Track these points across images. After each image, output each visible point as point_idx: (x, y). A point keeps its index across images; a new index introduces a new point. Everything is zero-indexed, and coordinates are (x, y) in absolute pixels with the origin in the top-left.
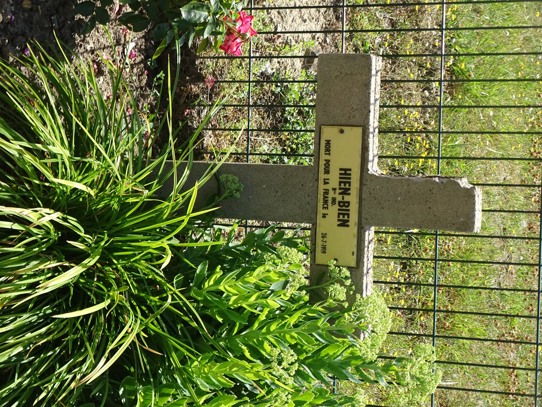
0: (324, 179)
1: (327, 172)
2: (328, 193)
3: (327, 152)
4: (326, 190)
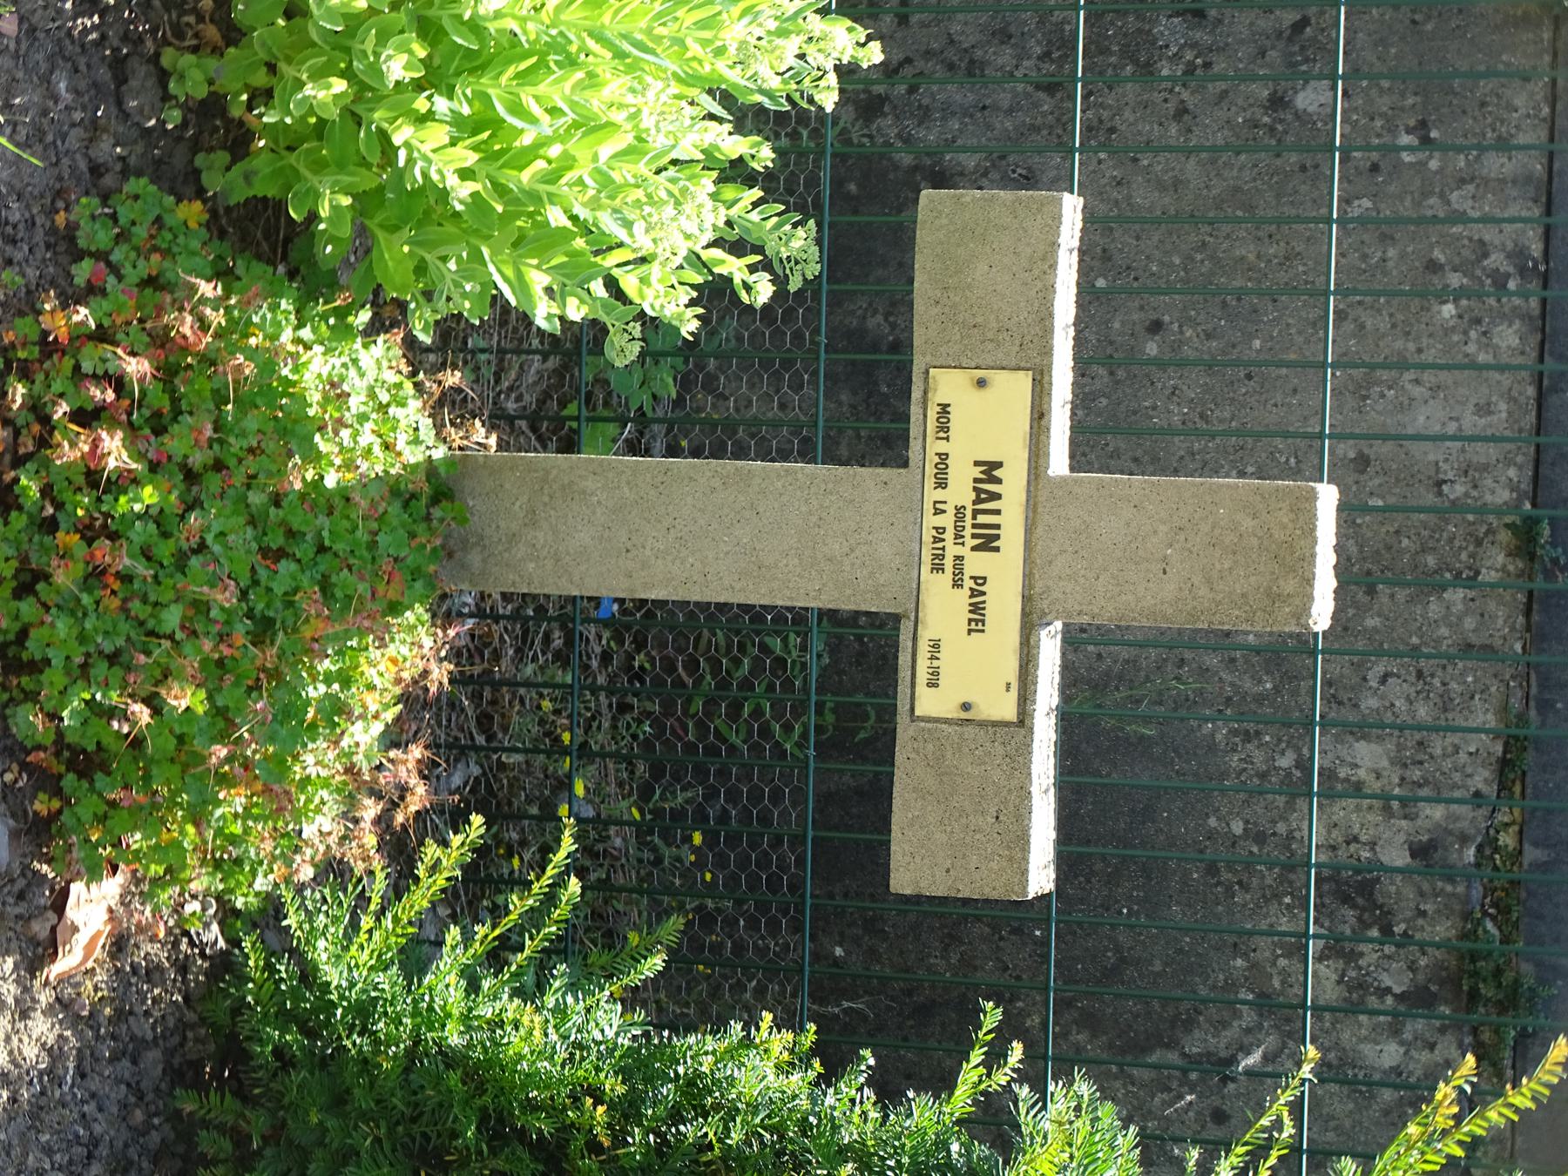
1: (942, 484)
3: (942, 435)
4: (936, 528)
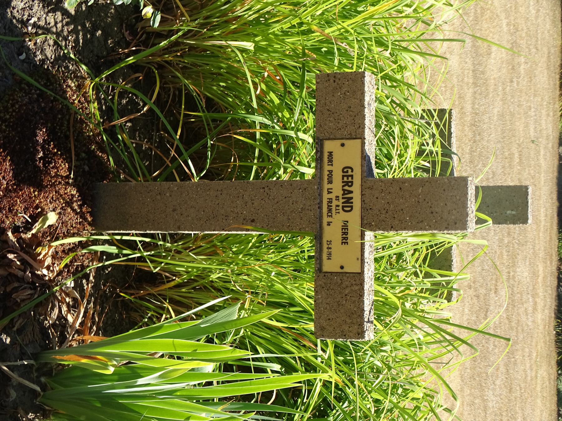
0: (328, 189)
1: (330, 182)
2: (331, 202)
3: (330, 163)
4: (330, 199)
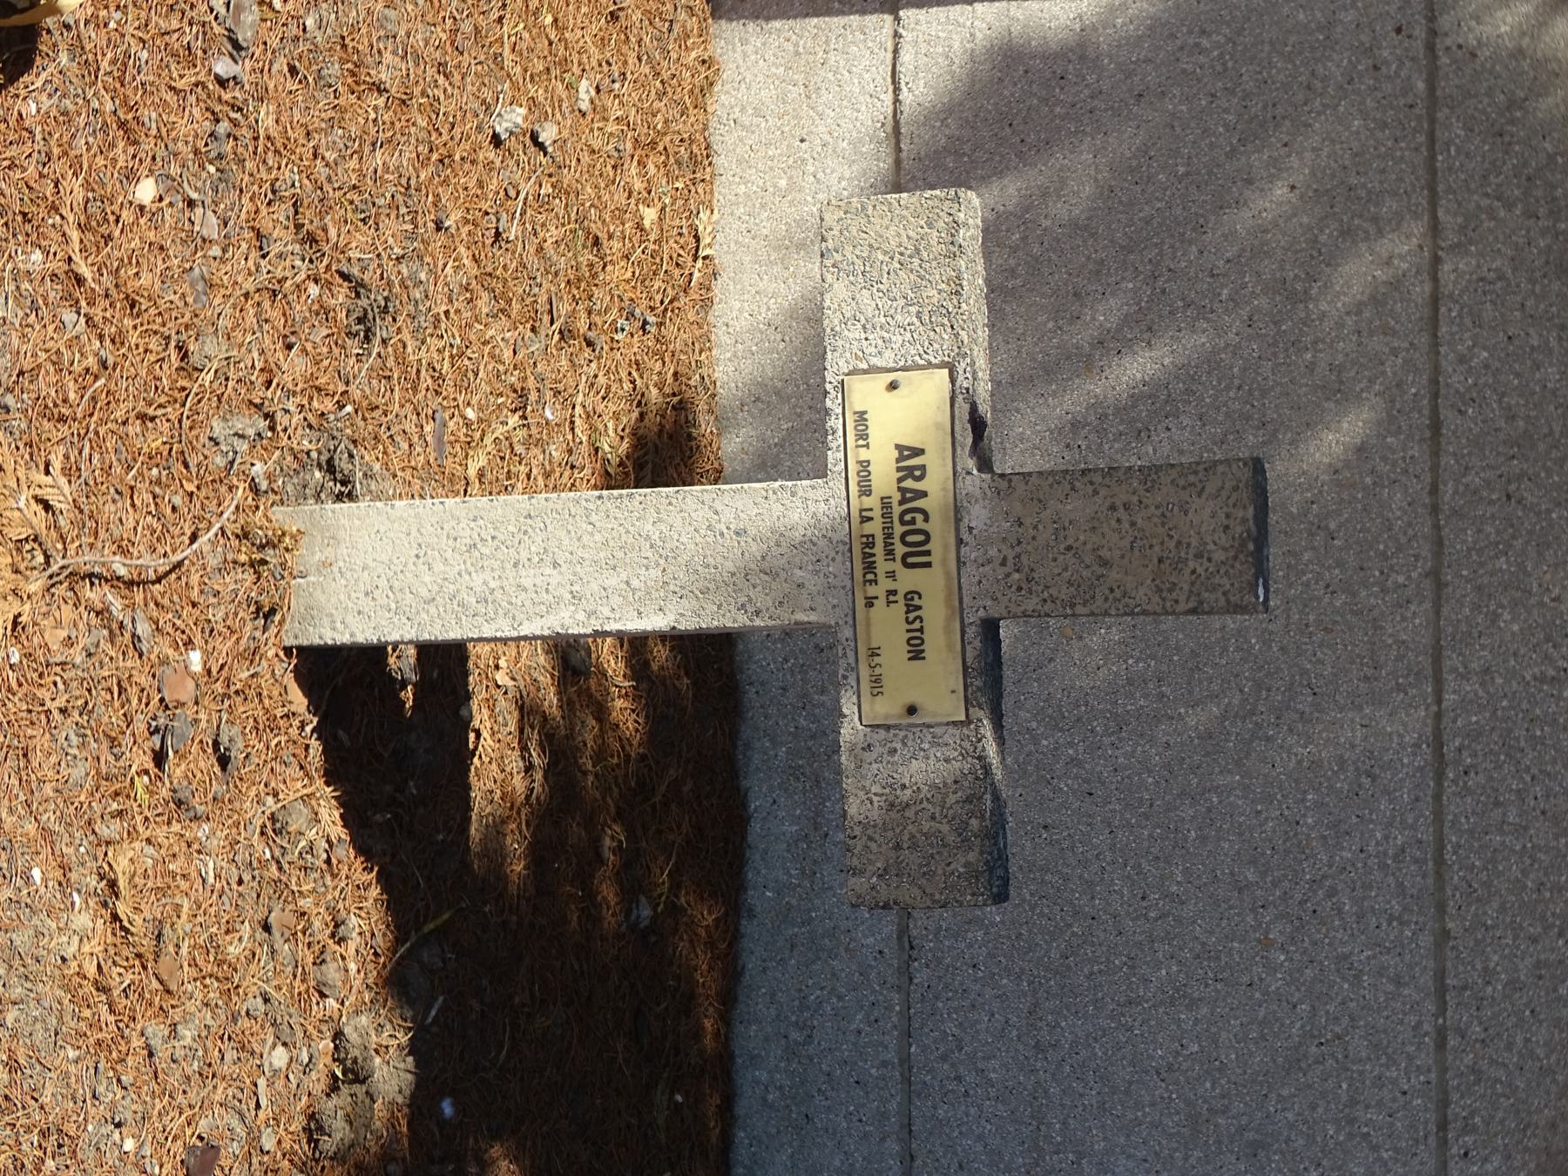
0: (861, 510)
2: (871, 545)
3: (861, 442)
4: (867, 536)
